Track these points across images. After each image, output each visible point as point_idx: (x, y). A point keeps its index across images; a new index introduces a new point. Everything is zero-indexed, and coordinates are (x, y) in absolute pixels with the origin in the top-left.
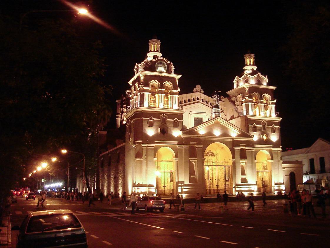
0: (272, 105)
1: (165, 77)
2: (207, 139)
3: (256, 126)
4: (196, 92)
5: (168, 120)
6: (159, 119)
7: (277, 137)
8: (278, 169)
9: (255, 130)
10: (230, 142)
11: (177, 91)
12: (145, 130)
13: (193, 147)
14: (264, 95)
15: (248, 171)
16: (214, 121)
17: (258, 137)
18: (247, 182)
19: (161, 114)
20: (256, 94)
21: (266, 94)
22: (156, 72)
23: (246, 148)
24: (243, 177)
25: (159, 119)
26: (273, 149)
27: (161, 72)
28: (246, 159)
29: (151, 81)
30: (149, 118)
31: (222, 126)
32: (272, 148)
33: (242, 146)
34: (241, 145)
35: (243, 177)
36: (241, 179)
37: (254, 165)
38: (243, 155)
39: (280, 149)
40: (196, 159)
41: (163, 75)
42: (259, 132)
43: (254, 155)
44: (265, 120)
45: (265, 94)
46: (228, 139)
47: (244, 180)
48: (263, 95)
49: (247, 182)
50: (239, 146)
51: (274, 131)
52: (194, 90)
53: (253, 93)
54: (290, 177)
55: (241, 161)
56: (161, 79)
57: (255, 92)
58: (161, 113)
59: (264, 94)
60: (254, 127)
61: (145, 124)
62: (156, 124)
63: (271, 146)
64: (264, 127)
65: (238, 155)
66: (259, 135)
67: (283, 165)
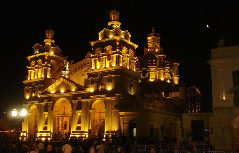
0: (113, 55)
1: (39, 56)
2: (57, 96)
3: (93, 79)
4: (87, 57)
5: (36, 86)
6: (31, 87)
7: (113, 86)
8: (112, 117)
9: (92, 83)
10: (71, 96)
11: (44, 64)
12: (25, 96)
13: (47, 104)
14: (106, 47)
15: (82, 121)
16: (60, 81)
17: (94, 89)
18: (81, 130)
19: (32, 83)
20: (99, 49)
21: (108, 46)
22: (33, 55)
23: (82, 100)
24: (79, 125)
25: (31, 87)
26: (107, 98)
27: (37, 54)
28: (81, 110)
29: (32, 62)
30: (27, 88)
31: (66, 84)
32: (106, 97)
33: (79, 99)
34: (77, 98)
35: (79, 125)
36: (77, 127)
37: (88, 115)
38: (79, 107)
39: (114, 98)
40: (48, 112)
41: (38, 55)
42: (96, 84)
43: (89, 106)
44: (102, 72)
45: (107, 46)
46: (69, 94)
47: (79, 128)
48: (106, 48)
49: (81, 130)
50: (76, 99)
51: (110, 81)
52: (86, 57)
53: (97, 49)
54: (129, 125)
55: (77, 112)
56: (36, 59)
57: (98, 48)
58: (32, 83)
59: (106, 46)
60: (92, 80)
61: (25, 91)
62: (30, 90)
63: (104, 95)
64: (101, 79)
65: (75, 107)
66: (96, 87)
67: (120, 113)
